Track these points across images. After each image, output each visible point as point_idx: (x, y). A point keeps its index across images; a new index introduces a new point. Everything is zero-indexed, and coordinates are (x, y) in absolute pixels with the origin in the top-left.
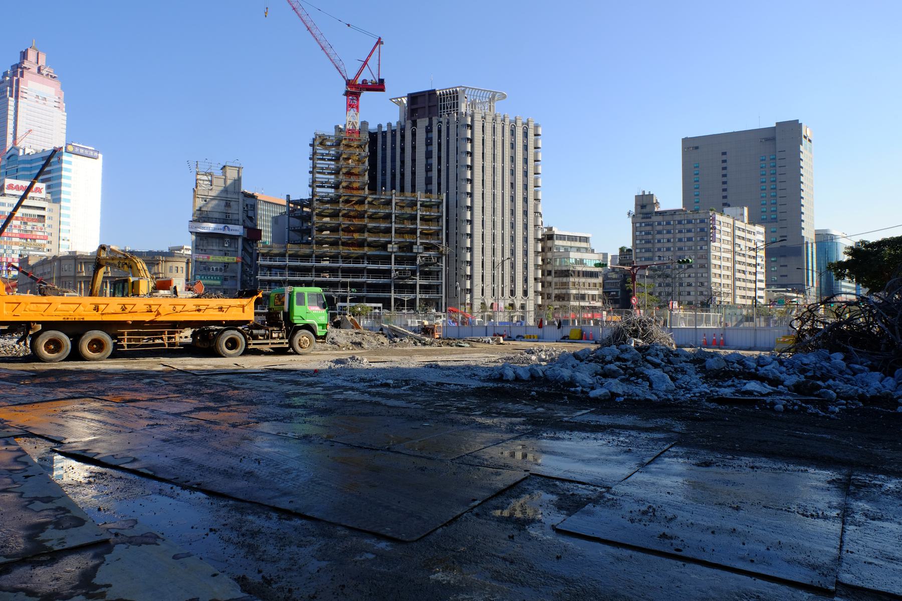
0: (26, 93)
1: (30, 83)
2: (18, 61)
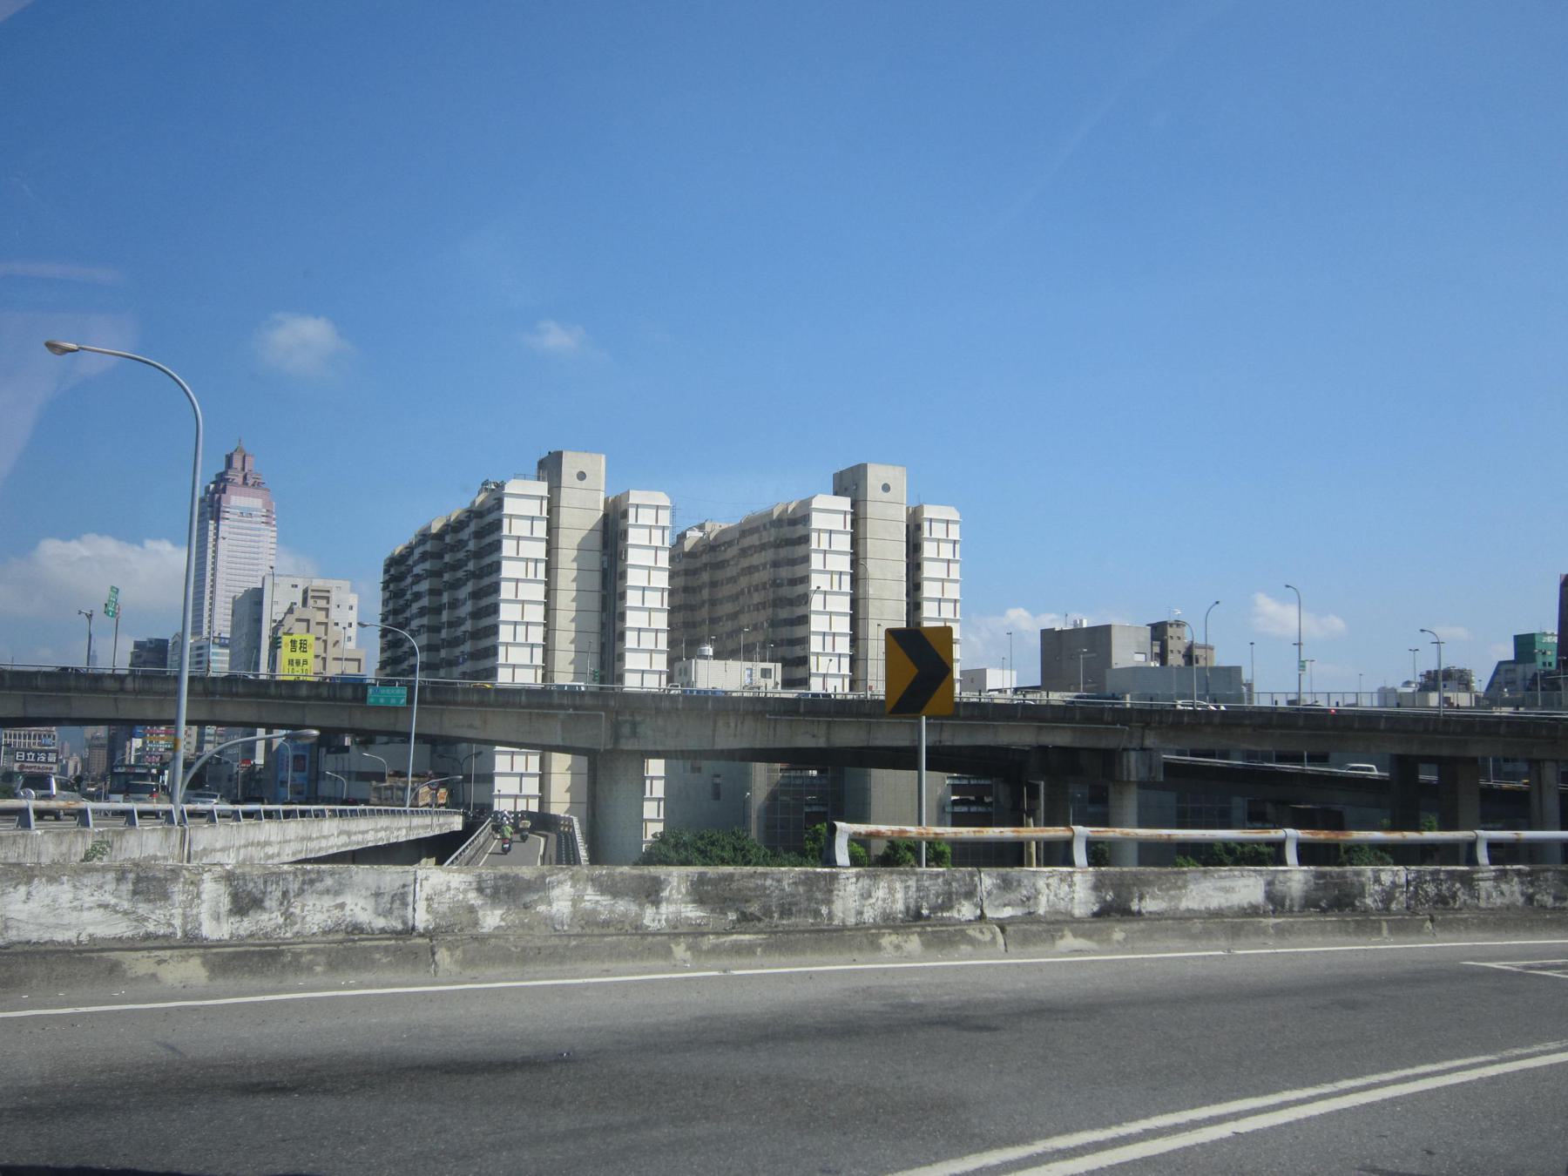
0: (228, 512)
1: (233, 498)
2: (222, 469)
